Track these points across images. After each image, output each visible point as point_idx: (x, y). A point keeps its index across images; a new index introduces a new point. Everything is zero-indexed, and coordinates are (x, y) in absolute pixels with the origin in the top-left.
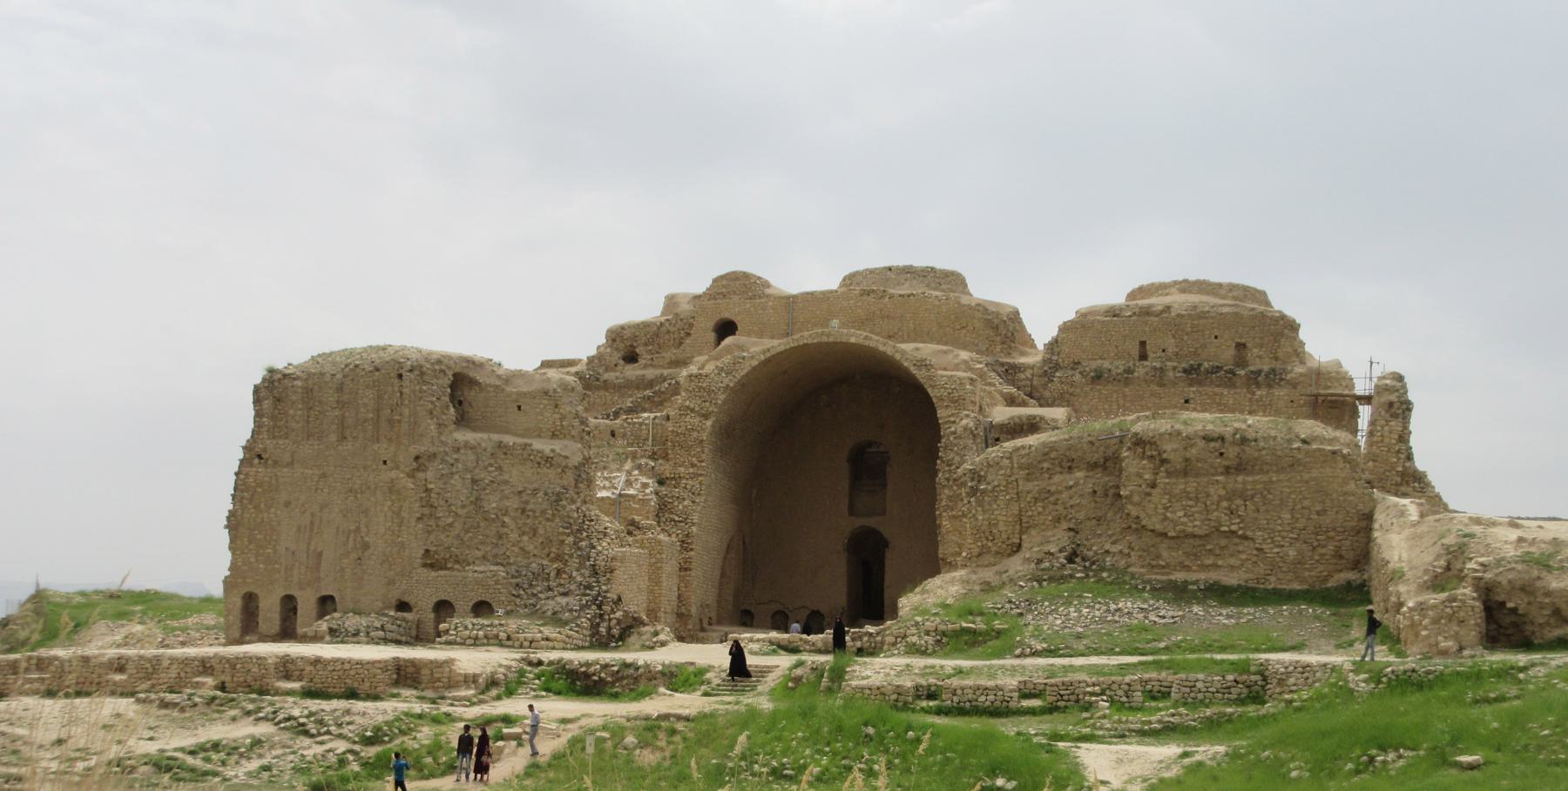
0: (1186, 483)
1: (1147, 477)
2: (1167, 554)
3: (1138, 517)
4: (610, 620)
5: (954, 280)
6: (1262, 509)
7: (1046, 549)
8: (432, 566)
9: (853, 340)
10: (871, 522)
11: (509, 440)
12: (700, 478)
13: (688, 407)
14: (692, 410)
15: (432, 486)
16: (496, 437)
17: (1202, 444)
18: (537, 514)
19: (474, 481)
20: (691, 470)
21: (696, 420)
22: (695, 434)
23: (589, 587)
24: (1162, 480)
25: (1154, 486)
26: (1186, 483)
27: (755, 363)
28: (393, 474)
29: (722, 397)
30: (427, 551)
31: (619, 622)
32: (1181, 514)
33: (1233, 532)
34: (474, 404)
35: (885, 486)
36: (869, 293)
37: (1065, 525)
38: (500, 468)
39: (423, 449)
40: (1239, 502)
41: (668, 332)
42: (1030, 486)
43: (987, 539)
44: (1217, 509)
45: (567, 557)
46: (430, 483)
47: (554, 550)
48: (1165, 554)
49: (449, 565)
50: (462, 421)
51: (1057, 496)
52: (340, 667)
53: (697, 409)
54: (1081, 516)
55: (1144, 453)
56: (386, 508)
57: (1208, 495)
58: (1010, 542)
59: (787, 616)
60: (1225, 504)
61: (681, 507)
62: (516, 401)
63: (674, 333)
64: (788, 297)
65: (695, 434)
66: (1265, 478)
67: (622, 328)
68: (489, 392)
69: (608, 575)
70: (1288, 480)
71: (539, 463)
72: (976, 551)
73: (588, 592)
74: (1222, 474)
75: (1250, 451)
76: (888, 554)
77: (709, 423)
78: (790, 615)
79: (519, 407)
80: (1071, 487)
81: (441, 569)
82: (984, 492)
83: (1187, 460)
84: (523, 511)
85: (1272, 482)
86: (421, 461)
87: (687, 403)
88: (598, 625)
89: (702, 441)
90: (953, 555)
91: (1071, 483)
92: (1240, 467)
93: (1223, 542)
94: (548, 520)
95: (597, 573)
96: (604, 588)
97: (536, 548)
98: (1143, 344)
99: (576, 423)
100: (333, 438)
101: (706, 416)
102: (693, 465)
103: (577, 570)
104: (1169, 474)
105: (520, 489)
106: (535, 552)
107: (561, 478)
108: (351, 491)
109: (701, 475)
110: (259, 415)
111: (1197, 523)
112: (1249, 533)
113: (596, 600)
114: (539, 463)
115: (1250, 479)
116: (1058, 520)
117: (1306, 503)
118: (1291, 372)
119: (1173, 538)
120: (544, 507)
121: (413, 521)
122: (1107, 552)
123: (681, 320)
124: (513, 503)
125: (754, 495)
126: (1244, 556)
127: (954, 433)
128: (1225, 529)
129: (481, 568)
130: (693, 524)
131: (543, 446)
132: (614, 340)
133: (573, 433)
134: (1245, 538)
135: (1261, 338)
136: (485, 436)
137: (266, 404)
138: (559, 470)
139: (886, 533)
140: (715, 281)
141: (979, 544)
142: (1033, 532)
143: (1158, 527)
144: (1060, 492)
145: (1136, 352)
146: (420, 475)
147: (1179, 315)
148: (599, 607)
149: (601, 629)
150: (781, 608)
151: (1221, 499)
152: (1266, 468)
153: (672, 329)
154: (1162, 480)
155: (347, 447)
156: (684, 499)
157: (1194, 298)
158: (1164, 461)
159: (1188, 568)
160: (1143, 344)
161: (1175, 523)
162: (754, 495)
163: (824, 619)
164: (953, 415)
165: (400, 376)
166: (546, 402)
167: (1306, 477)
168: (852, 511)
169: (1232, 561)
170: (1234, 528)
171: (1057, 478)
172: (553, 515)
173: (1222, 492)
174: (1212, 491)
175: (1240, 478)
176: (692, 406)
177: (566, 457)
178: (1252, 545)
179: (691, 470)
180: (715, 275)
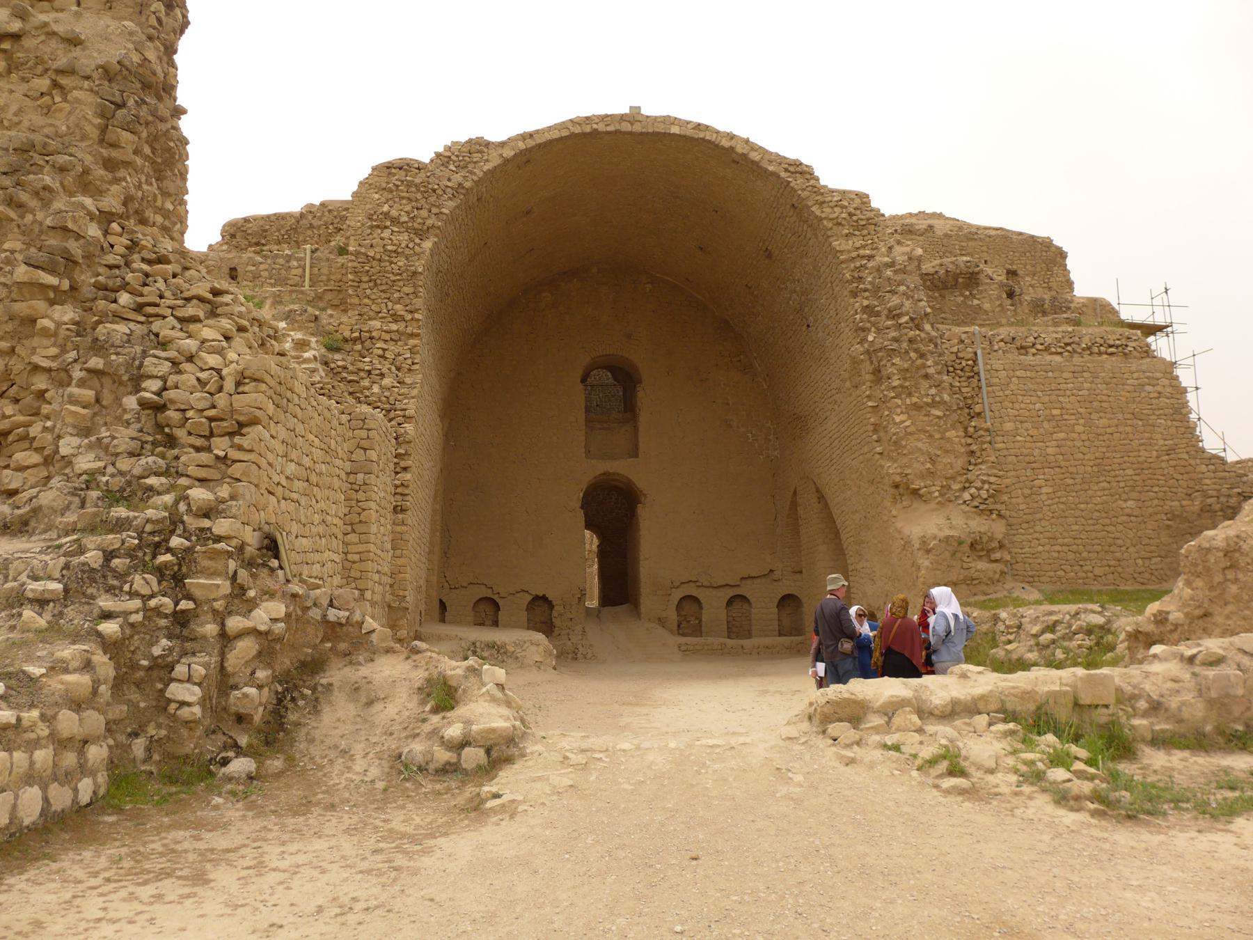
4: (226, 639)
10: (621, 467)
12: (412, 342)
13: (386, 215)
14: (395, 221)
20: (394, 327)
21: (404, 237)
22: (402, 262)
23: (133, 492)
27: (508, 153)
29: (448, 206)
31: (268, 643)
41: (311, 227)
53: (404, 218)
61: (376, 389)
63: (319, 227)
65: (402, 262)
67: (246, 220)
69: (221, 446)
73: (121, 512)
76: (643, 512)
77: (427, 245)
78: (501, 603)
87: (386, 208)
88: (163, 669)
89: (415, 273)
90: (922, 477)
95: (171, 442)
96: (199, 494)
101: (421, 233)
102: (396, 318)
103: (85, 432)
109: (412, 335)
113: (157, 548)
123: (330, 211)
127: (892, 264)
130: (408, 418)
132: (233, 236)
135: (1034, 266)
147: (946, 235)
148: (175, 579)
149: (177, 691)
150: (489, 594)
153: (316, 222)
156: (382, 375)
164: (864, 247)
168: (588, 453)
176: (394, 213)
179: (394, 327)
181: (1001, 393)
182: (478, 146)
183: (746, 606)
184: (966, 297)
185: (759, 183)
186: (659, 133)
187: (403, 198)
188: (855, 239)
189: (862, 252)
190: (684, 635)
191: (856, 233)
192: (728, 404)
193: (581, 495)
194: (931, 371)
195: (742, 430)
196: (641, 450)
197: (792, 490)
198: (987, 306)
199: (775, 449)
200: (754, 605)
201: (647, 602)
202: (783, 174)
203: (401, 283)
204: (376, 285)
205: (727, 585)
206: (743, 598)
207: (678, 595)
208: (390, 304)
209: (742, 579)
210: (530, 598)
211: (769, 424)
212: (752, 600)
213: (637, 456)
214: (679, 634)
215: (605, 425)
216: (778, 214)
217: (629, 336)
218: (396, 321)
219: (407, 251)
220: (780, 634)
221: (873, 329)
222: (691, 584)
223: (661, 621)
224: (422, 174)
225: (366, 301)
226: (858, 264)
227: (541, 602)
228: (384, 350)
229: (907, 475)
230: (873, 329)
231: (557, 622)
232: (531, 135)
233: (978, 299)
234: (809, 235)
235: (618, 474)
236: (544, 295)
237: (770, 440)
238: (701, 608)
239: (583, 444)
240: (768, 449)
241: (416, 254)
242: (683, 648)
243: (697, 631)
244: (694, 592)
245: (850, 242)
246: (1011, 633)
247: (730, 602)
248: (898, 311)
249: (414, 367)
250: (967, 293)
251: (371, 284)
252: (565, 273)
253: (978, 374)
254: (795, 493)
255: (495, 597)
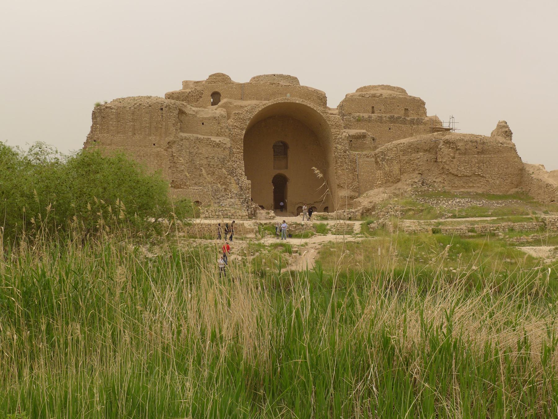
0: (465, 157)
1: (452, 155)
2: (457, 182)
3: (448, 169)
5: (295, 80)
6: (489, 167)
7: (414, 180)
8: (175, 187)
9: (297, 102)
10: (282, 172)
11: (199, 136)
13: (235, 126)
14: (237, 127)
15: (175, 154)
16: (195, 135)
17: (470, 144)
18: (215, 166)
19: (190, 153)
20: (238, 150)
23: (241, 195)
24: (457, 156)
25: (454, 158)
26: (465, 157)
28: (158, 149)
29: (248, 122)
30: (173, 181)
32: (463, 168)
33: (479, 175)
34: (183, 122)
36: (272, 84)
37: (417, 172)
38: (198, 148)
39: (171, 139)
40: (482, 164)
41: (192, 96)
42: (404, 158)
43: (389, 177)
44: (474, 167)
45: (228, 184)
46: (174, 153)
47: (222, 180)
48: (456, 182)
49: (182, 187)
50: (182, 130)
51: (413, 161)
52: (200, 227)
54: (423, 168)
55: (450, 146)
56: (155, 163)
57: (472, 162)
58: (397, 178)
60: (477, 165)
61: (236, 165)
62: (202, 121)
63: (195, 96)
64: (241, 84)
66: (490, 156)
68: (190, 117)
70: (497, 157)
71: (214, 146)
72: (384, 181)
74: (476, 154)
75: (486, 147)
76: (289, 184)
77: (244, 132)
79: (203, 124)
80: (419, 158)
81: (178, 188)
82: (388, 160)
83: (466, 149)
84: (209, 165)
85: (492, 158)
86: (170, 144)
87: (235, 124)
90: (343, 184)
91: (419, 157)
92: (482, 152)
93: (476, 178)
94: (220, 169)
97: (214, 180)
98: (373, 107)
99: (227, 131)
100: (130, 134)
101: (242, 129)
104: (460, 154)
105: (207, 156)
106: (214, 181)
107: (223, 152)
108: (139, 156)
110: (95, 123)
111: (468, 171)
112: (484, 175)
113: (245, 200)
114: (214, 146)
115: (485, 156)
116: (414, 170)
117: (502, 165)
118: (424, 119)
119: (460, 177)
120: (218, 163)
121: (167, 169)
122: (435, 182)
124: (205, 162)
126: (482, 183)
127: (341, 138)
128: (477, 173)
129: (196, 188)
131: (217, 140)
133: (226, 134)
134: (483, 177)
135: (413, 107)
136: (191, 135)
137: (98, 119)
138: (222, 149)
140: (210, 76)
141: (386, 179)
142: (405, 175)
143: (455, 173)
144: (414, 160)
145: (371, 110)
146: (170, 150)
147: (386, 98)
148: (247, 203)
151: (476, 163)
152: (490, 152)
153: (194, 94)
154: (457, 156)
155: (137, 137)
157: (390, 92)
158: (457, 150)
159: (464, 187)
160: (373, 107)
161: (461, 172)
164: (338, 131)
165: (162, 109)
166: (215, 121)
167: (503, 156)
169: (478, 185)
170: (480, 173)
171: (413, 155)
172: (222, 167)
173: (476, 161)
174: (473, 160)
175: (482, 156)
177: (225, 144)
178: (485, 179)
179: (238, 150)
180: (210, 74)
198: (367, 143)
201: (289, 208)
202: (321, 113)
207: (297, 206)
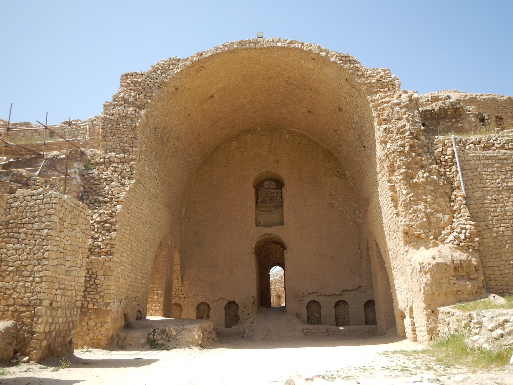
12: (131, 163)
14: (126, 101)
20: (122, 155)
27: (188, 63)
35: (280, 206)
59: (209, 307)
78: (211, 306)
109: (132, 160)
125: (183, 214)
130: (119, 203)
139: (285, 239)
162: (183, 214)
163: (238, 308)
164: (384, 97)
181: (472, 174)
182: (174, 62)
183: (346, 307)
184: (453, 122)
185: (327, 69)
186: (270, 47)
187: (132, 90)
188: (380, 93)
189: (384, 100)
190: (311, 323)
191: (382, 90)
192: (332, 195)
193: (254, 246)
194: (425, 163)
195: (340, 208)
196: (285, 221)
197: (366, 240)
199: (359, 218)
200: (350, 306)
202: (338, 62)
203: (128, 133)
204: (115, 134)
205: (334, 295)
206: (344, 302)
207: (307, 300)
208: (122, 144)
209: (343, 291)
210: (226, 303)
211: (355, 205)
212: (349, 304)
213: (283, 225)
214: (308, 322)
215: (268, 209)
216: (340, 86)
217: (278, 162)
218: (124, 153)
219: (132, 116)
220: (367, 323)
221: (389, 141)
222: (314, 294)
223: (298, 316)
224: (143, 77)
225: (109, 143)
226: (382, 107)
227: (233, 305)
228: (115, 167)
229: (412, 226)
230: (389, 141)
231: (240, 315)
232: (201, 54)
233: (462, 123)
234: (357, 95)
235: (274, 235)
236: (233, 143)
237: (356, 214)
238: (321, 308)
239: (254, 219)
240: (355, 218)
241: (136, 117)
242: (305, 331)
243: (319, 321)
244: (315, 298)
245: (378, 95)
246: (477, 328)
247: (337, 304)
248: (402, 130)
249: (132, 176)
250: (454, 120)
251: (112, 134)
252: (243, 131)
253: (456, 163)
254: (367, 241)
255: (208, 302)
